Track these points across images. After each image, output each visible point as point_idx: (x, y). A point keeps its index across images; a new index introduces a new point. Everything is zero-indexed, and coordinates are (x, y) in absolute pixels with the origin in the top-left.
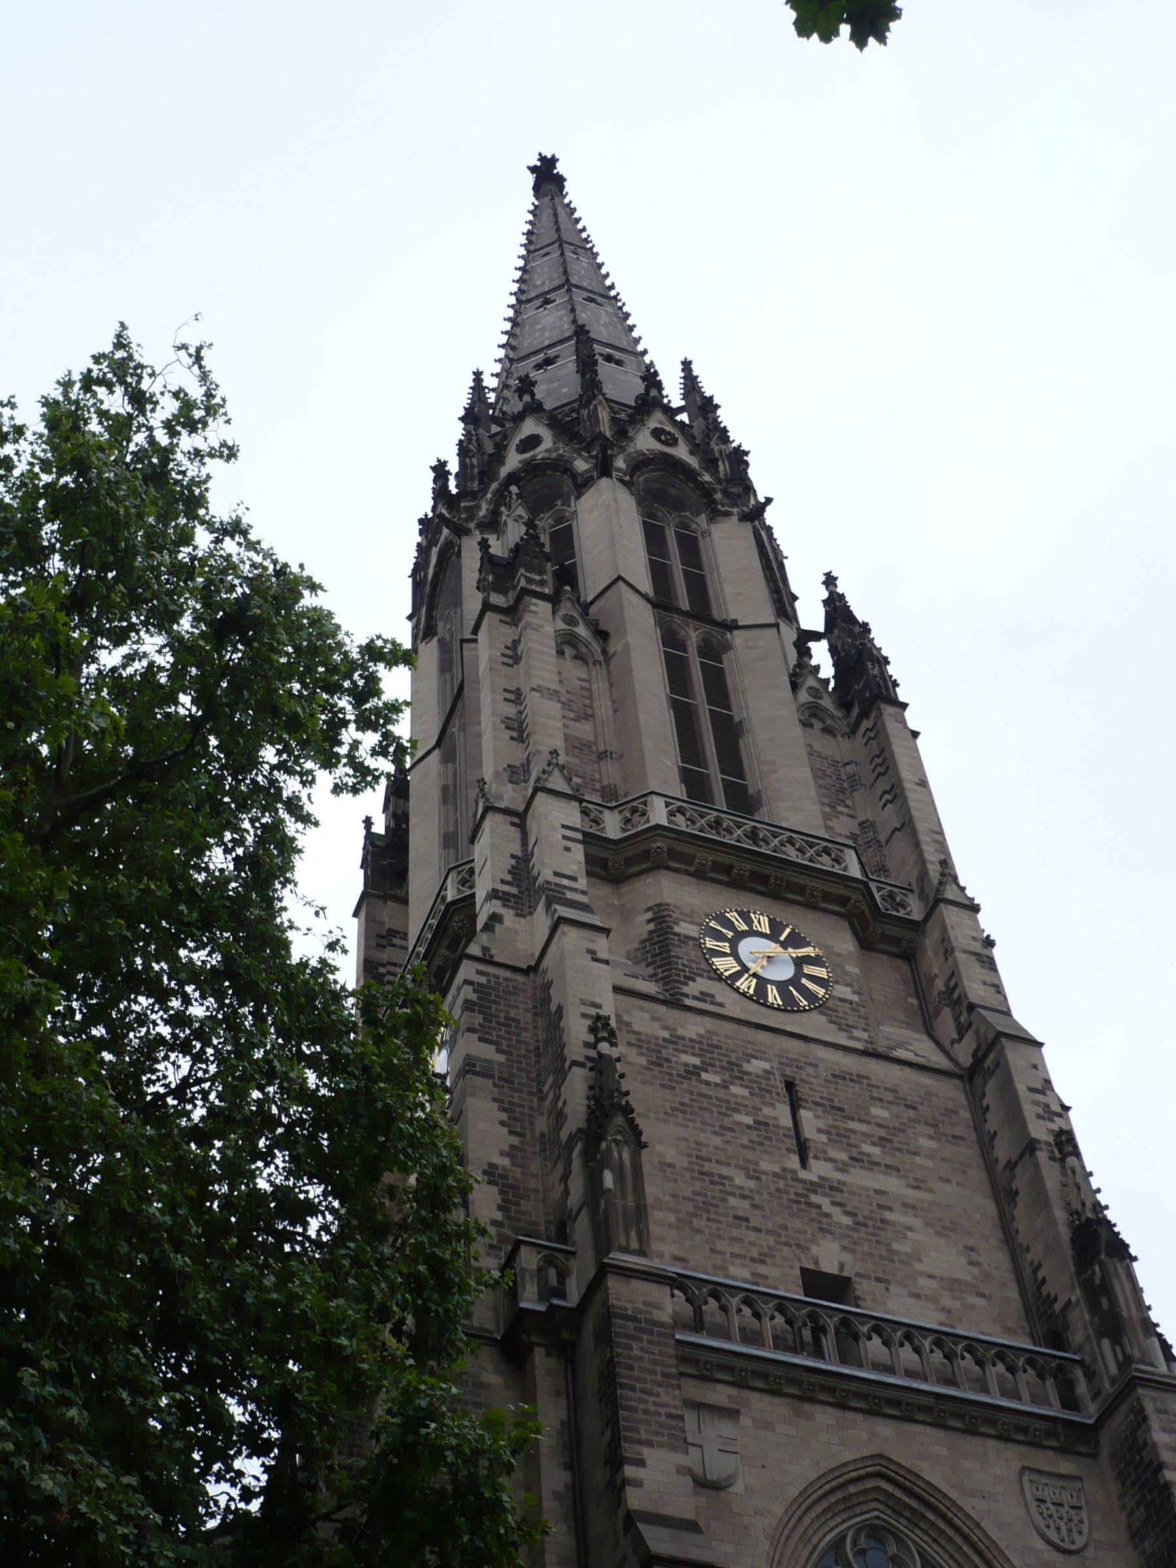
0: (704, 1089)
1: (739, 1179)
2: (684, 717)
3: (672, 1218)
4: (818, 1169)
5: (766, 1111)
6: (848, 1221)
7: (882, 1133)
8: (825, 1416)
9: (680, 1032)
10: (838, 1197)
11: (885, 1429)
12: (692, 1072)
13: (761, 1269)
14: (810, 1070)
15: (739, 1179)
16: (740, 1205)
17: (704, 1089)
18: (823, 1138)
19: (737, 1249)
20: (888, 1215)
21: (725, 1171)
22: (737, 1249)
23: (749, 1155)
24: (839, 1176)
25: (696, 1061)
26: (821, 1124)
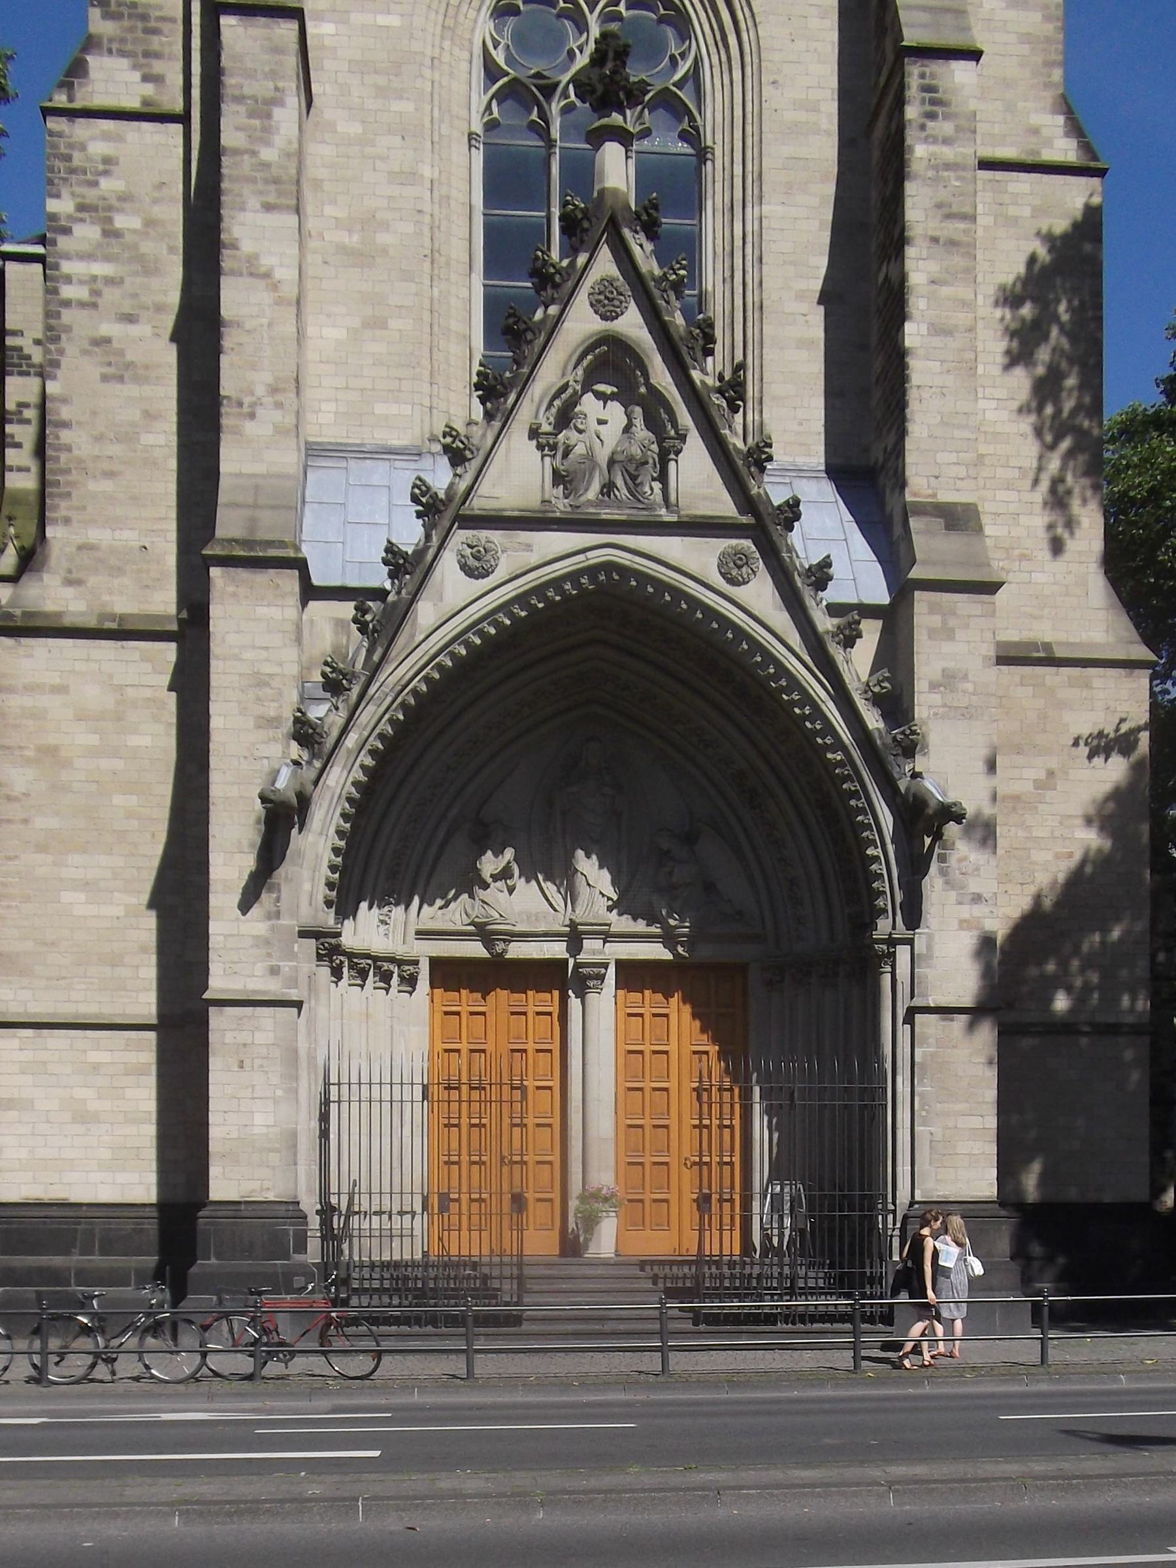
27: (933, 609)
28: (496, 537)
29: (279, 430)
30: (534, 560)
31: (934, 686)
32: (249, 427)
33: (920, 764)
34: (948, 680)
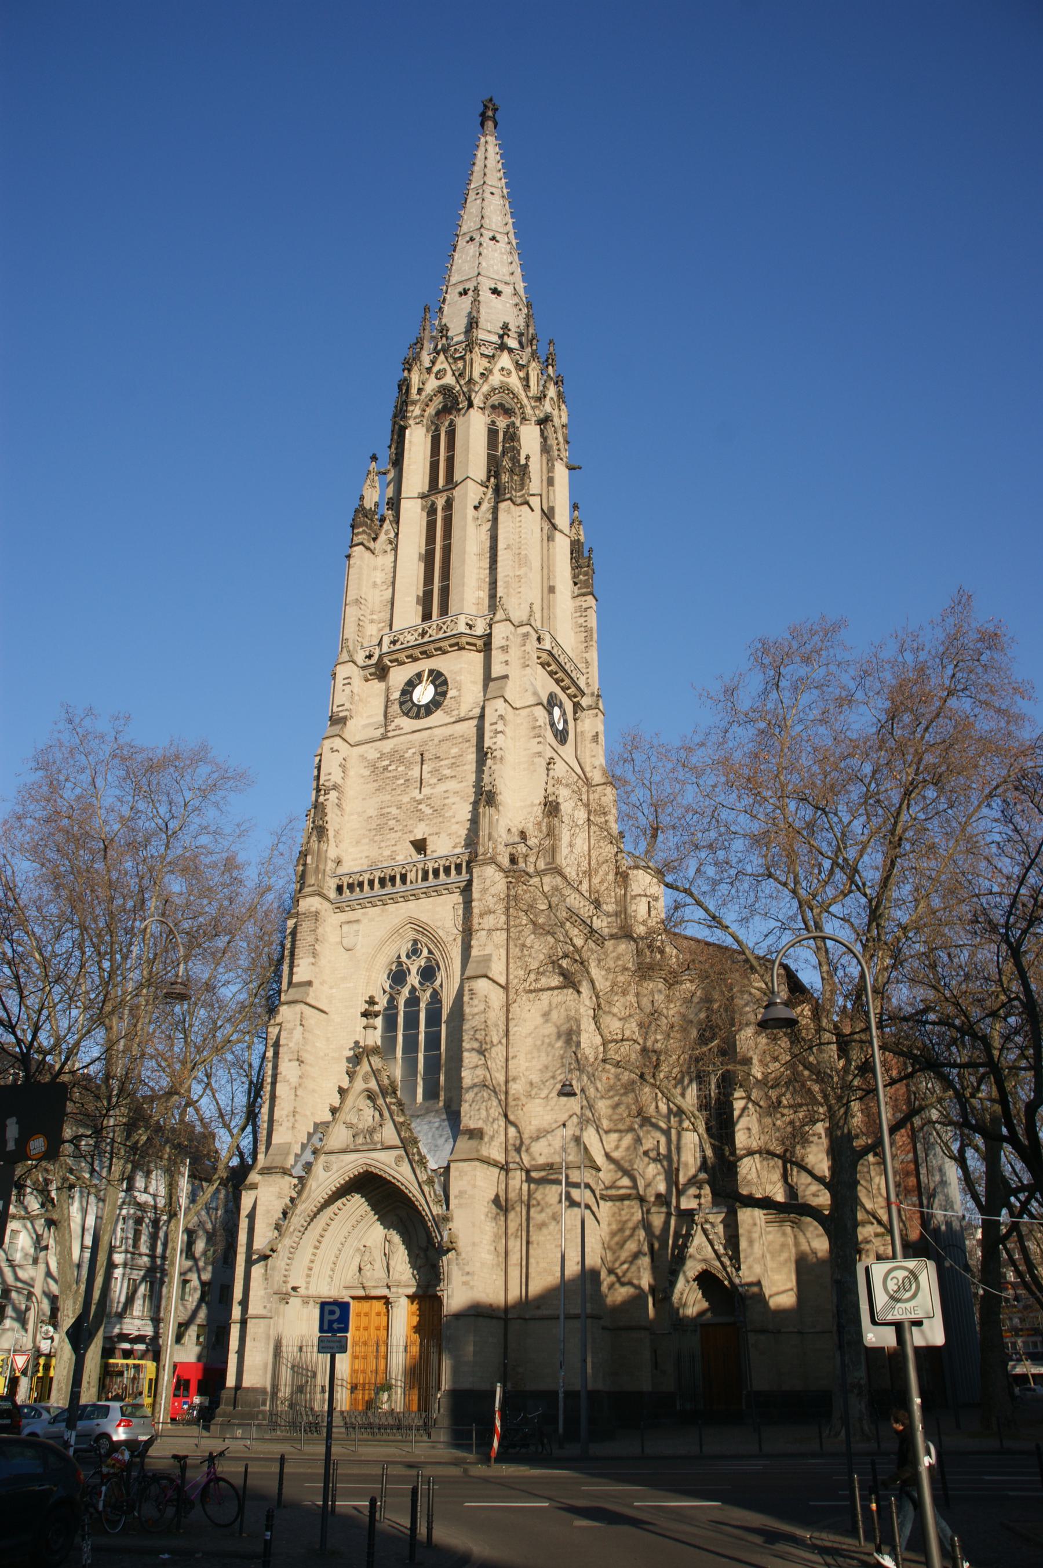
0: (389, 775)
1: (394, 811)
2: (428, 558)
3: (367, 840)
4: (426, 791)
5: (410, 773)
6: (431, 811)
7: (453, 761)
8: (391, 907)
9: (385, 751)
10: (429, 802)
11: (412, 905)
12: (385, 768)
13: (394, 848)
14: (430, 743)
15: (394, 811)
16: (392, 823)
17: (389, 775)
18: (429, 775)
19: (388, 843)
20: (447, 801)
21: (388, 810)
22: (388, 843)
23: (400, 798)
24: (432, 791)
25: (387, 762)
26: (430, 769)
27: (457, 1168)
28: (333, 1157)
29: (288, 1129)
30: (343, 1164)
31: (456, 1197)
32: (280, 1129)
33: (450, 1225)
34: (461, 1194)
